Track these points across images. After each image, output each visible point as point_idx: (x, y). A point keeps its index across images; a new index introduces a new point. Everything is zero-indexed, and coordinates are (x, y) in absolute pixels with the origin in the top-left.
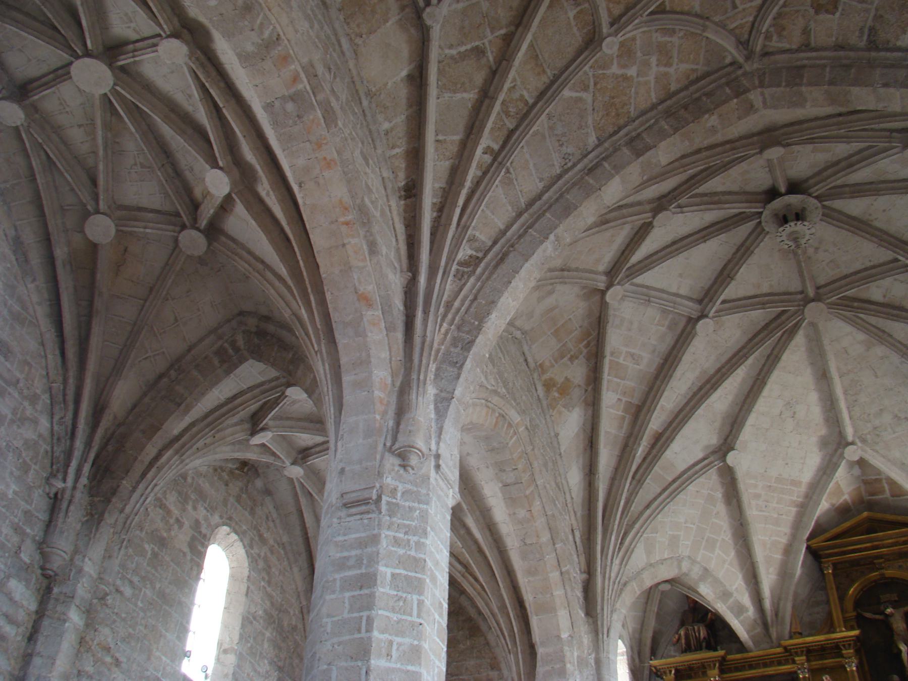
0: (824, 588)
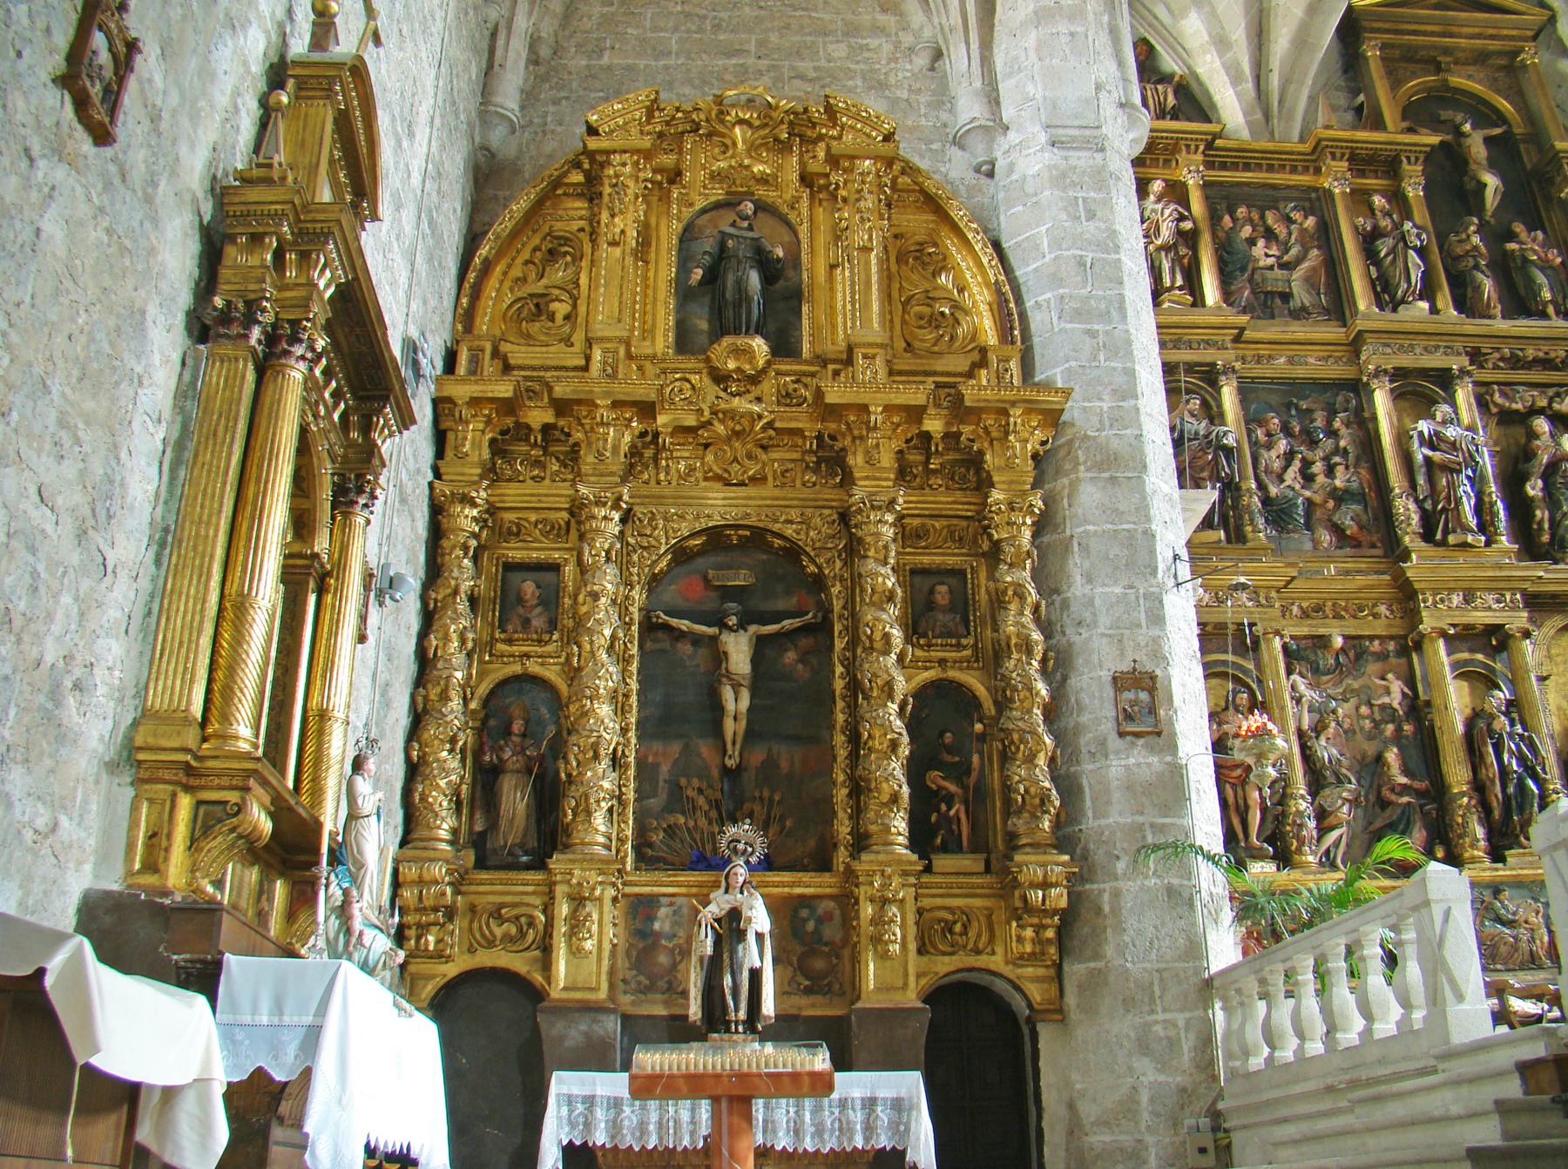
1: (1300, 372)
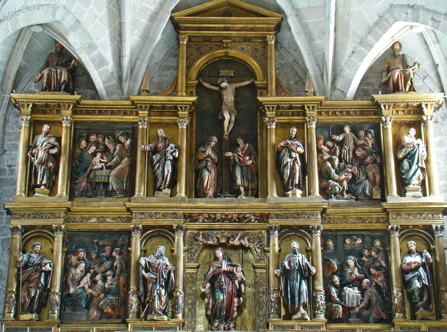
0: (177, 56)
1: (102, 226)
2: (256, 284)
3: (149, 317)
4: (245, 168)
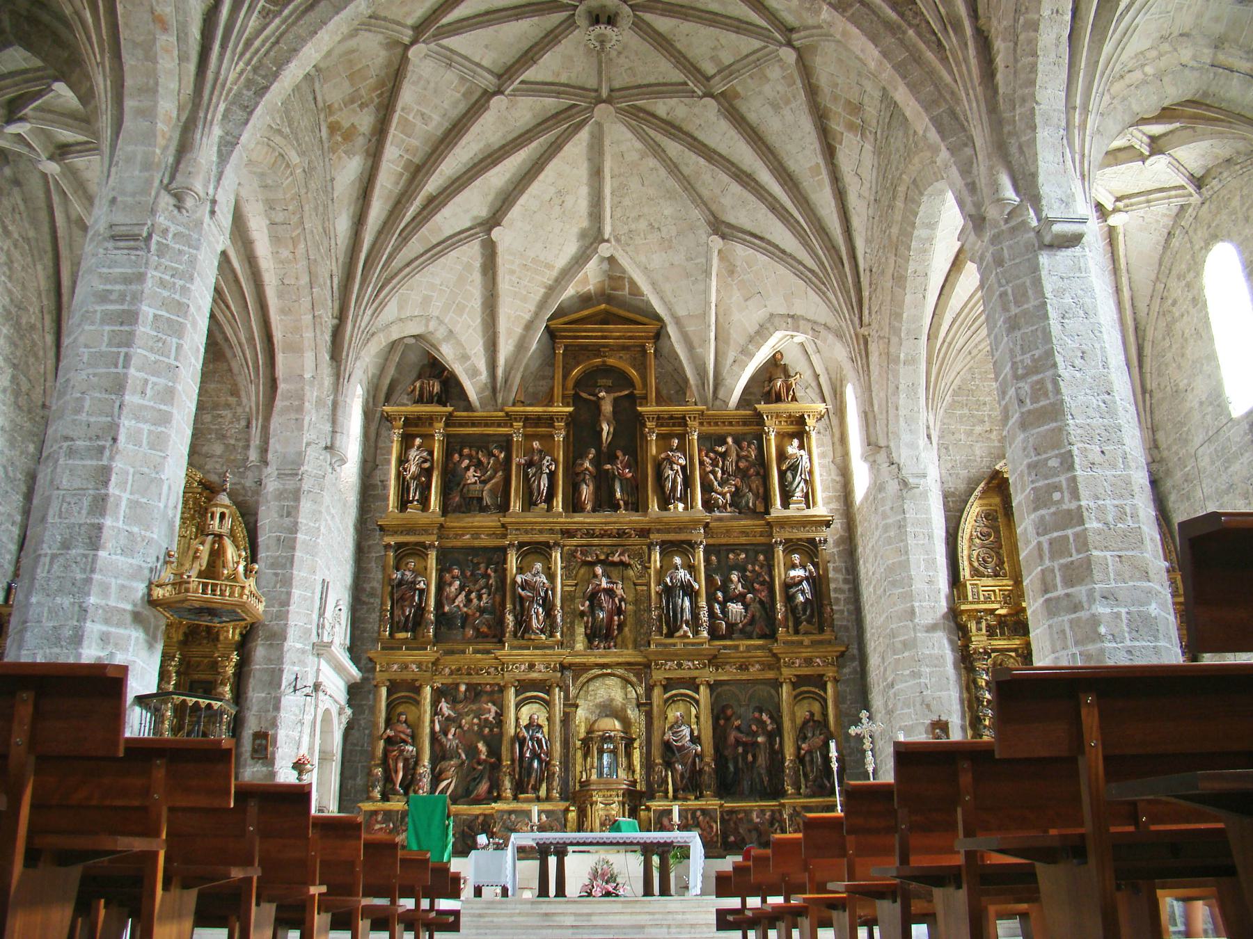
0: (552, 365)
1: (477, 543)
2: (636, 602)
3: (526, 636)
4: (624, 482)
